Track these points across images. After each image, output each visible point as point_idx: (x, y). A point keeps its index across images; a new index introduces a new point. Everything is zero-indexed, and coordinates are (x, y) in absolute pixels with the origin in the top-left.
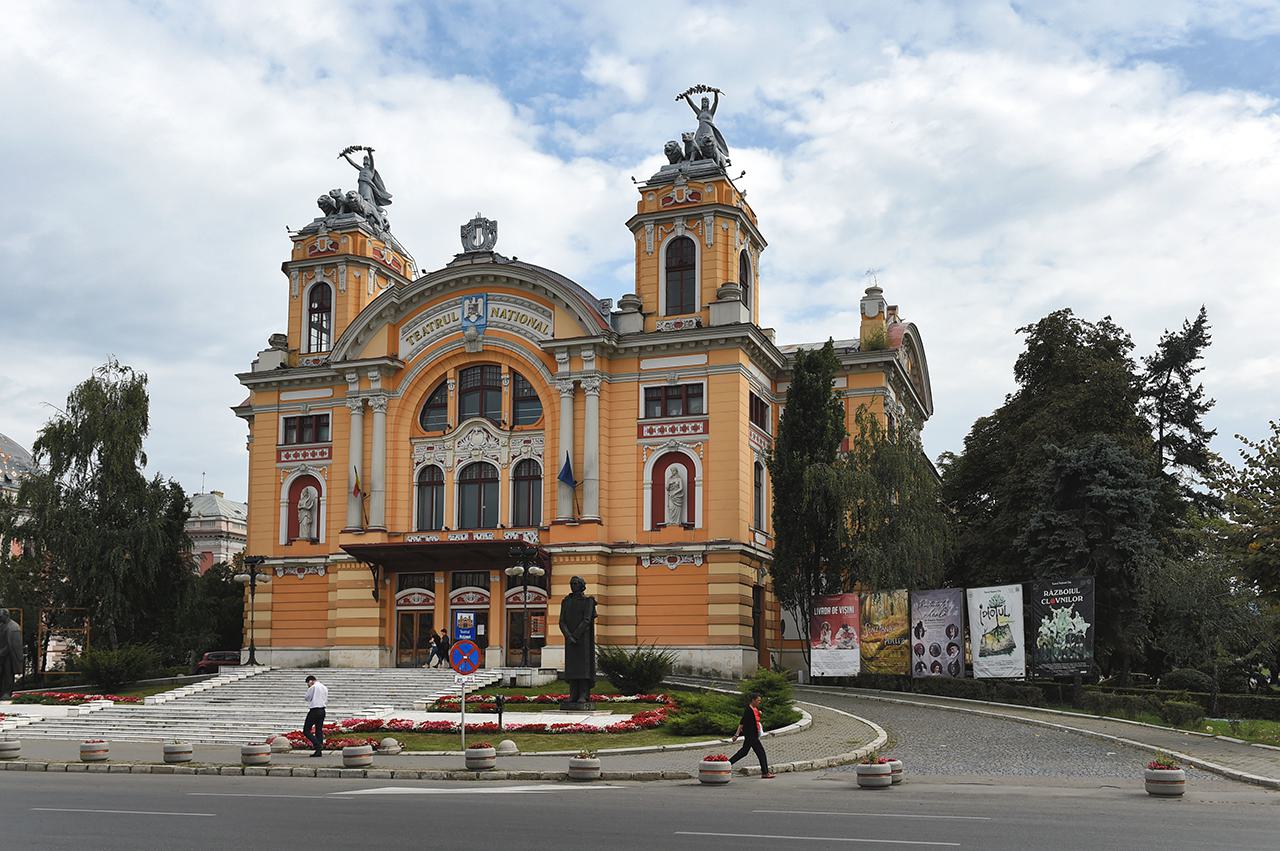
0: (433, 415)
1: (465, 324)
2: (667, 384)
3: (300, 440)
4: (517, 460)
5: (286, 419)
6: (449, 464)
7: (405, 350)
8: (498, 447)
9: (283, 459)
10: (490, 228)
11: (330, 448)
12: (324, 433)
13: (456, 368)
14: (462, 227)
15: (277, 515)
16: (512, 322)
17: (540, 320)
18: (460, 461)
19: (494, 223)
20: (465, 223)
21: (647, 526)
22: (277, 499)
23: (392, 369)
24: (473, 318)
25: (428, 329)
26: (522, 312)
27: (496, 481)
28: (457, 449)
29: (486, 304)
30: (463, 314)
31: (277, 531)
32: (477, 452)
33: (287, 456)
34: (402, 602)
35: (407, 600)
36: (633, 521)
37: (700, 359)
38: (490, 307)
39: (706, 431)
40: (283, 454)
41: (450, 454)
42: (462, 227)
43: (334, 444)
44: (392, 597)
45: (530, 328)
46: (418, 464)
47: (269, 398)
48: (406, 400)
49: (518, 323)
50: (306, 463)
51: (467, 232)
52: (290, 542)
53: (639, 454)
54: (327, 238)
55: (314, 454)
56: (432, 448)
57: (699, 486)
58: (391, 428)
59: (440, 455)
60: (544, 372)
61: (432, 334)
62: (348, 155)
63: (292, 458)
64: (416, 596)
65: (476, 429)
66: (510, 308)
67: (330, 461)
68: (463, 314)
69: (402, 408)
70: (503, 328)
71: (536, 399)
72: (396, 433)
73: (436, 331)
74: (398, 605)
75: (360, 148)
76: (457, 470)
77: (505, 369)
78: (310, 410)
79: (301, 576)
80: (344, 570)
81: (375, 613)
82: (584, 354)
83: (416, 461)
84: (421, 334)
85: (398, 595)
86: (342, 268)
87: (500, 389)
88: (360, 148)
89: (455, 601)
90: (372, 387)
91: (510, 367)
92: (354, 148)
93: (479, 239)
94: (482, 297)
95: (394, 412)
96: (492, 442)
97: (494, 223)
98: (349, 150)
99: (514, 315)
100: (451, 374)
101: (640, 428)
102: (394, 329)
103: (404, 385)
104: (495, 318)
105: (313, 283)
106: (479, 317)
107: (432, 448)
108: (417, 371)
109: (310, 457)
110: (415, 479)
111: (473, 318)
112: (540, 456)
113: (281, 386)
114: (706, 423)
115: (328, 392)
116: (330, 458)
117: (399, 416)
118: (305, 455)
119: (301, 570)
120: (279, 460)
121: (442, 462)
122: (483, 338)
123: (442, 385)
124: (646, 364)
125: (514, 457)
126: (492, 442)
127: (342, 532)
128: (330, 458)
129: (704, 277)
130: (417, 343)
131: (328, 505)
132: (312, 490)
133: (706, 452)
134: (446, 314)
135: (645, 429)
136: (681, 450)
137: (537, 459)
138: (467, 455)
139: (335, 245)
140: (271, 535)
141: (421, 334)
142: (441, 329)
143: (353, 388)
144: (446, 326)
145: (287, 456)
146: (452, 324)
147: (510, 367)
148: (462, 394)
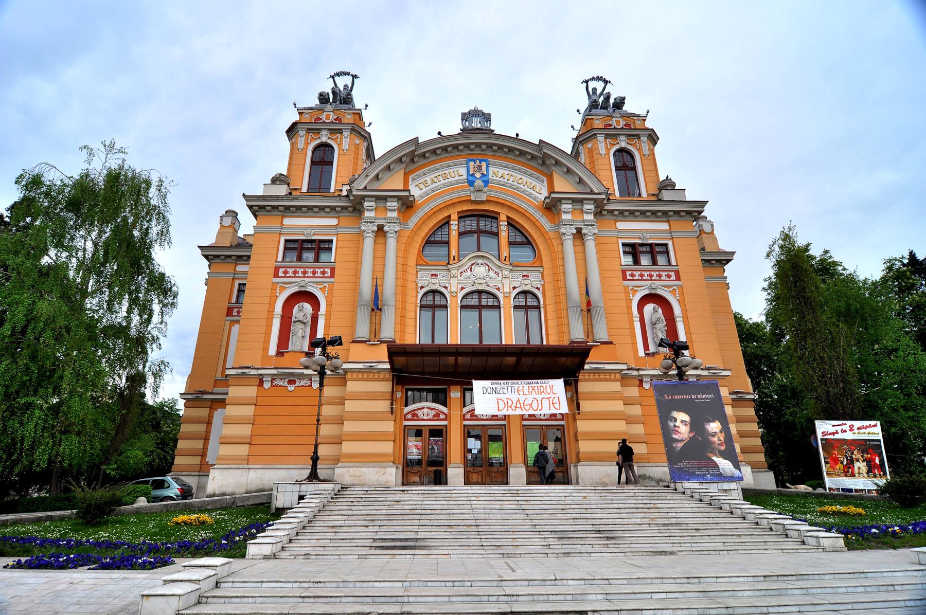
0: (430, 250)
1: (471, 178)
2: (639, 241)
3: (300, 259)
4: (517, 291)
5: (286, 241)
6: (454, 289)
7: (415, 191)
8: (498, 279)
9: (281, 274)
10: (487, 118)
11: (333, 270)
12: (324, 256)
13: (458, 213)
14: (463, 114)
15: (269, 326)
16: (510, 182)
17: (534, 183)
18: (462, 288)
19: (489, 115)
20: (467, 111)
21: (641, 353)
22: (271, 311)
23: (407, 205)
24: (478, 175)
25: (436, 180)
26: (519, 176)
27: (498, 307)
28: (459, 277)
29: (487, 167)
30: (468, 171)
31: (267, 342)
32: (482, 281)
33: (286, 273)
34: (409, 416)
35: (415, 415)
36: (630, 347)
37: (664, 226)
38: (491, 169)
39: (678, 278)
40: (281, 270)
41: (454, 281)
42: (463, 114)
43: (336, 265)
44: (402, 410)
45: (525, 188)
46: (422, 287)
47: (272, 221)
48: (415, 232)
49: (515, 183)
50: (306, 280)
51: (465, 117)
52: (280, 354)
53: (627, 293)
54: (332, 113)
55: (314, 273)
56: (436, 275)
57: (680, 321)
58: (401, 253)
59: (445, 282)
60: (544, 222)
61: (438, 183)
62: (336, 78)
63: (291, 274)
64: (426, 411)
65: (480, 261)
66: (509, 172)
67: (331, 280)
68: (468, 171)
69: (411, 238)
70: (503, 185)
71: (528, 242)
72: (405, 258)
73: (443, 182)
74: (405, 420)
75: (348, 74)
76: (460, 295)
77: (503, 217)
78: (314, 234)
79: (291, 388)
80: (355, 380)
81: (389, 426)
82: (586, 207)
83: (420, 285)
84: (429, 182)
85: (407, 410)
86: (346, 133)
87: (496, 234)
88: (348, 74)
89: (468, 416)
90: (388, 215)
91: (508, 217)
92: (343, 73)
93: (476, 123)
94: (485, 161)
95: (404, 240)
96: (492, 274)
97: (489, 115)
98: (339, 74)
99: (512, 179)
100: (455, 217)
101: (624, 272)
102: (406, 175)
103: (414, 220)
104: (495, 178)
105: (318, 142)
106: (483, 175)
107: (436, 275)
108: (426, 209)
109: (310, 275)
110: (419, 302)
111: (478, 175)
112: (538, 288)
113: (287, 210)
114: (677, 273)
115: (334, 222)
116: (332, 276)
117: (409, 244)
118: (305, 273)
119: (292, 382)
120: (276, 275)
121: (446, 287)
122: (488, 190)
123: (446, 222)
124: (621, 225)
125: (514, 288)
126: (492, 274)
127: (354, 342)
128: (332, 276)
129: (646, 175)
130: (425, 189)
131: (328, 319)
132: (308, 307)
133: (682, 294)
134: (452, 170)
135: (628, 273)
136: (660, 292)
137: (536, 291)
138: (470, 282)
139: (339, 119)
140: (261, 345)
141: (429, 182)
142: (447, 181)
143: (367, 214)
144: (451, 179)
145: (286, 273)
146: (457, 178)
147: (508, 217)
148: (461, 234)
